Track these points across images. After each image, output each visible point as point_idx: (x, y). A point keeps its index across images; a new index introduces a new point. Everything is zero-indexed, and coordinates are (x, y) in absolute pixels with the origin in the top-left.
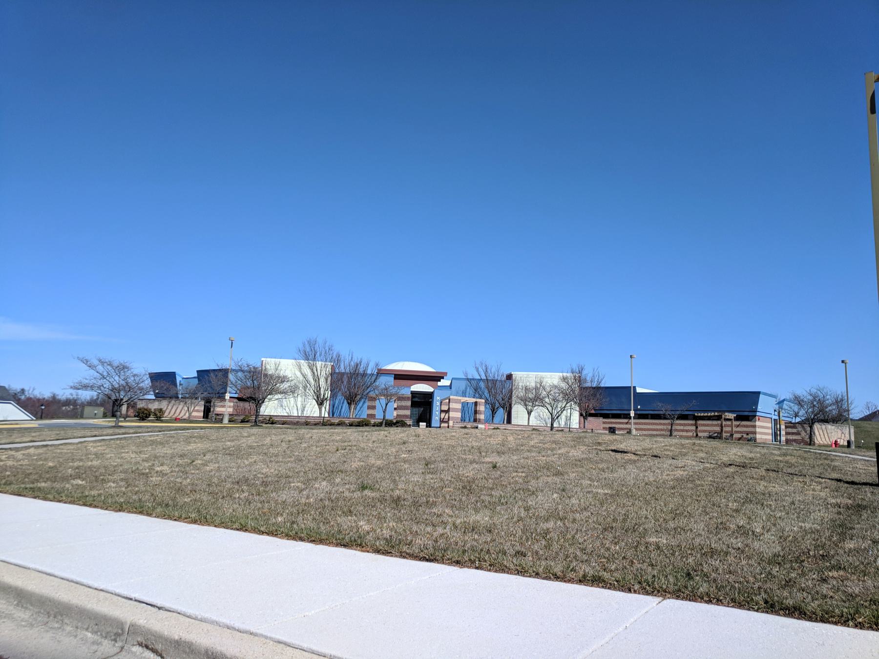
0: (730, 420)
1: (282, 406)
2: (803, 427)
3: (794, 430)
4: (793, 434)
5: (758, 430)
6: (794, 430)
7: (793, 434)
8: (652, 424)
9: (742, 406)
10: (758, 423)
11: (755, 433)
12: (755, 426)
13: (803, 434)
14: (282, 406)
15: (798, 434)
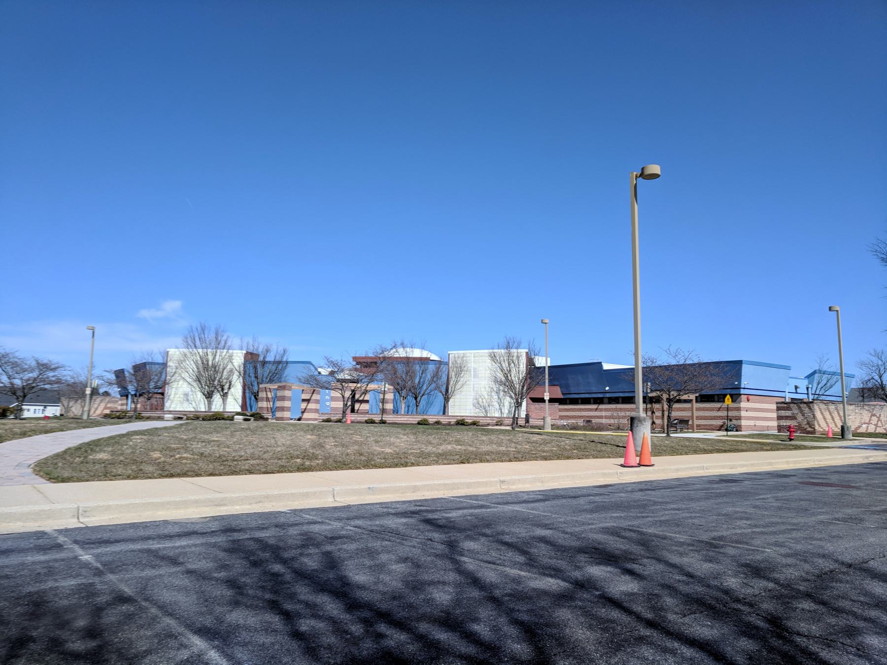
0: (690, 401)
1: (188, 400)
2: (800, 408)
3: (788, 413)
4: (787, 418)
5: (743, 414)
6: (788, 413)
7: (787, 418)
8: (573, 410)
9: (717, 385)
10: (744, 404)
11: (739, 418)
12: (739, 409)
13: (800, 417)
14: (188, 400)
15: (793, 418)
